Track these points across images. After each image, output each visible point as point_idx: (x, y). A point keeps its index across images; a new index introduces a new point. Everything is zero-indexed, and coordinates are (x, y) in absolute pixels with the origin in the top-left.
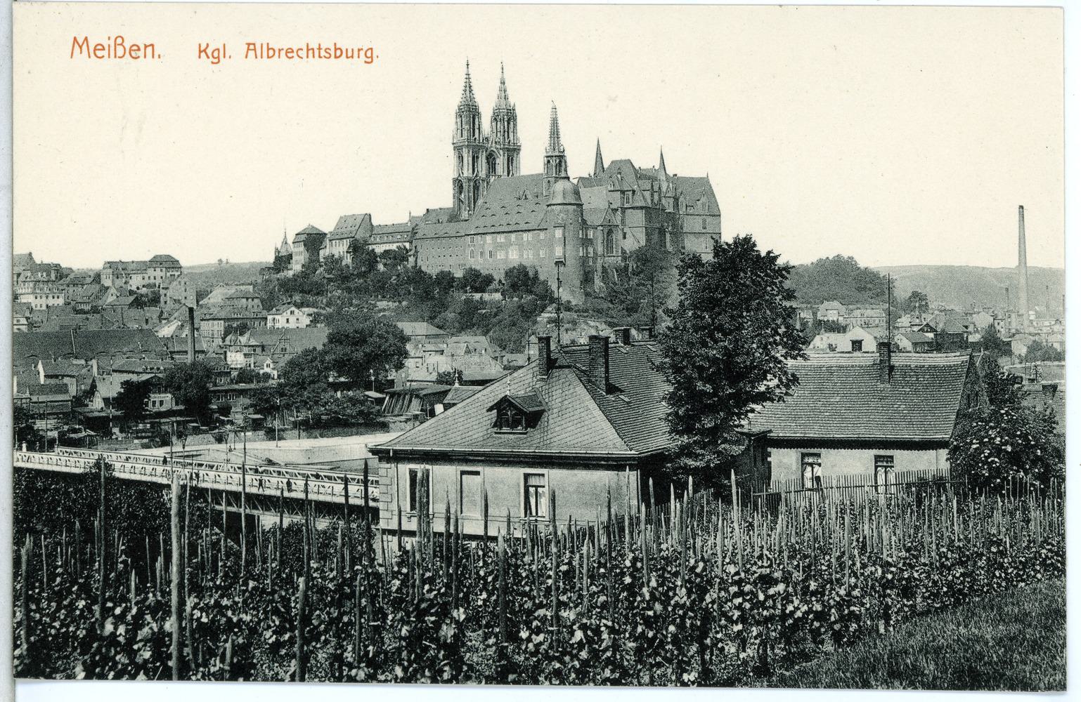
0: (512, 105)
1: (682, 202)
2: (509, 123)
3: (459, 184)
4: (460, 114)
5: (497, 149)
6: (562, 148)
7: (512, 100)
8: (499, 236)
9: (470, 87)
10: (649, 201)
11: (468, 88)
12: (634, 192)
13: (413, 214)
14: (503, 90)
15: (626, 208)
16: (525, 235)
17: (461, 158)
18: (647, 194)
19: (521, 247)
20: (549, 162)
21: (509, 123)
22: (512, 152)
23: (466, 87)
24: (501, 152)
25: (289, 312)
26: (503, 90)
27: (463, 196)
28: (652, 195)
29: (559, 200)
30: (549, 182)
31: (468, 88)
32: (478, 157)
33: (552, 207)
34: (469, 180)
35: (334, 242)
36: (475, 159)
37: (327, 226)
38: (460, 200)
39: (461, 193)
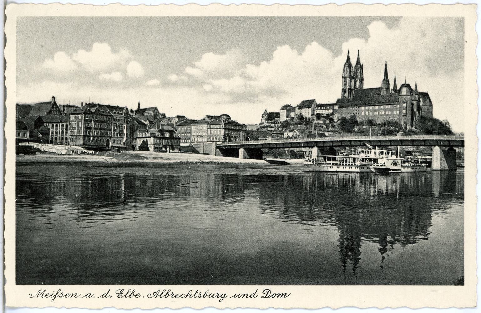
3: (344, 91)
7: (362, 62)
11: (348, 58)
14: (358, 59)
16: (387, 106)
22: (362, 80)
25: (294, 131)
26: (358, 59)
28: (418, 96)
29: (405, 94)
31: (348, 58)
33: (402, 96)
34: (349, 89)
36: (350, 82)
37: (294, 104)
39: (344, 94)
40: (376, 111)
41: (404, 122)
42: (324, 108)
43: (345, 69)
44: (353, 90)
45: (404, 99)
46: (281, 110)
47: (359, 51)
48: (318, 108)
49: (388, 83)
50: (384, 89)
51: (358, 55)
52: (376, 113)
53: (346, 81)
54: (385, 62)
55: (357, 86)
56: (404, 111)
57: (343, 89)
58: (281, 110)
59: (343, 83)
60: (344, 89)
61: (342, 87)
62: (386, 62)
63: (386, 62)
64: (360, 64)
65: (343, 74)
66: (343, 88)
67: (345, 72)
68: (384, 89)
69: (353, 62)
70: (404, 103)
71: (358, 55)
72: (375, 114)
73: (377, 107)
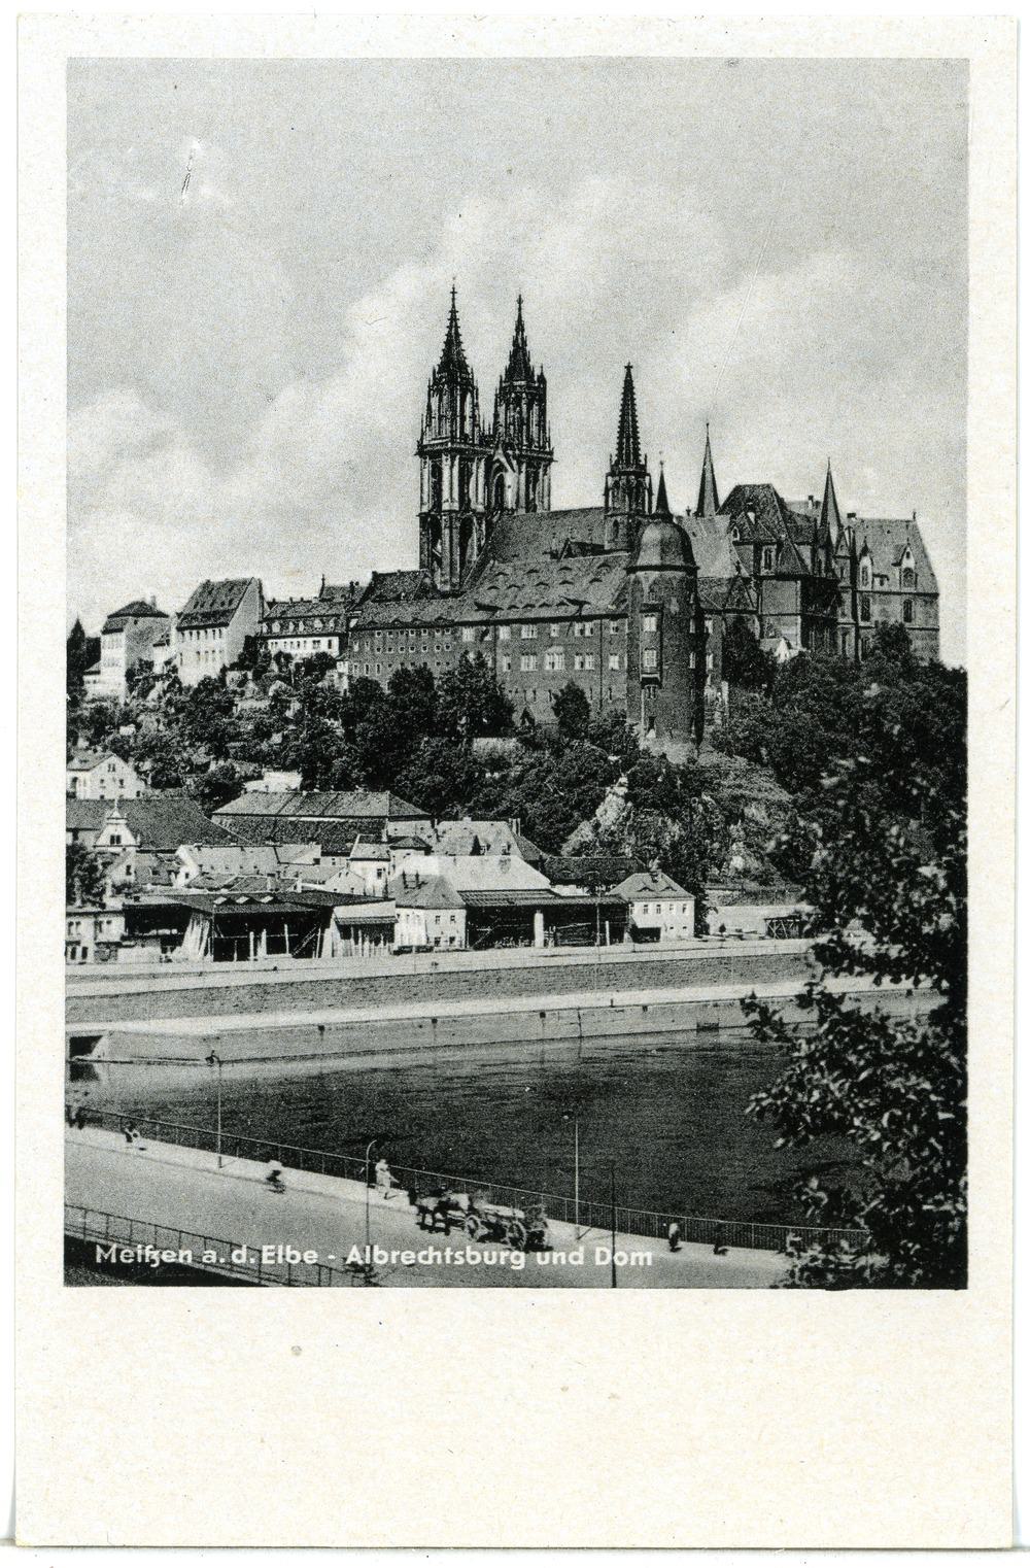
0: (537, 372)
1: (865, 569)
2: (530, 408)
3: (430, 525)
4: (435, 388)
5: (507, 456)
6: (642, 458)
7: (535, 362)
8: (524, 628)
9: (458, 335)
10: (808, 562)
11: (453, 341)
12: (780, 544)
13: (330, 582)
15: (764, 578)
16: (578, 627)
17: (437, 472)
18: (806, 552)
19: (571, 650)
20: (616, 484)
21: (530, 408)
22: (538, 460)
23: (449, 335)
24: (514, 462)
25: (105, 765)
27: (439, 547)
28: (814, 553)
29: (656, 561)
30: (616, 524)
31: (453, 341)
32: (470, 474)
35: (187, 632)
38: (433, 556)
39: (434, 546)
40: (528, 649)
41: (652, 720)
42: (297, 626)
43: (434, 407)
44: (479, 517)
45: (647, 590)
46: (106, 631)
47: (520, 301)
48: (270, 627)
49: (640, 484)
50: (619, 519)
51: (520, 327)
52: (528, 664)
53: (437, 472)
54: (623, 373)
55: (510, 497)
56: (649, 660)
57: (423, 517)
58: (106, 631)
59: (426, 481)
60: (427, 514)
61: (422, 504)
62: (629, 368)
63: (629, 368)
64: (528, 373)
65: (423, 433)
66: (425, 509)
67: (435, 422)
68: (619, 519)
69: (487, 365)
70: (650, 609)
71: (520, 327)
72: (523, 668)
73: (526, 632)
